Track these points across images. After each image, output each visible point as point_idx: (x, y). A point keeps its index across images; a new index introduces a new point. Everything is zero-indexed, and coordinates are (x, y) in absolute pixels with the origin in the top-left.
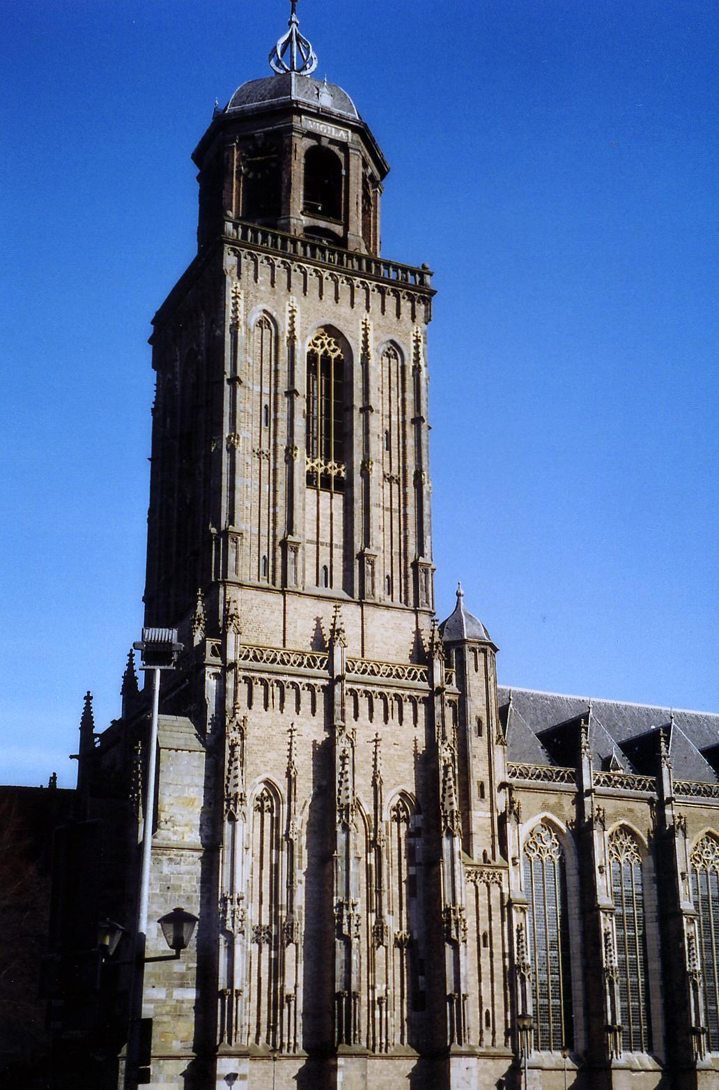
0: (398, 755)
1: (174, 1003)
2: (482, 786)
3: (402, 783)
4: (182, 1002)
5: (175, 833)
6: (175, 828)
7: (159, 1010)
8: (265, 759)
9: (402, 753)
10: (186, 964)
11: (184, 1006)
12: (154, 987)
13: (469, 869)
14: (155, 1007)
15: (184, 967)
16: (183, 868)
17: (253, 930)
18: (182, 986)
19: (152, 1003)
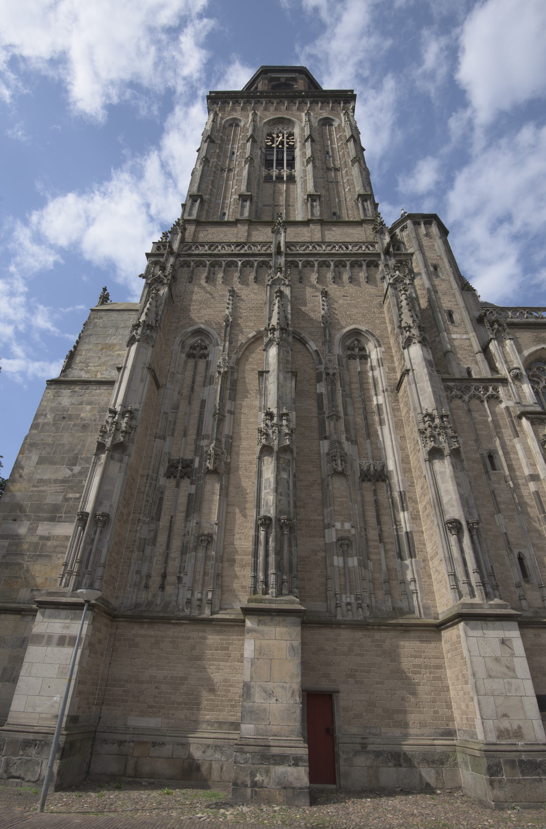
0: (348, 304)
1: (35, 539)
2: (450, 314)
3: (354, 323)
4: (48, 538)
5: (88, 372)
6: (89, 368)
7: (14, 548)
8: (200, 315)
9: (353, 302)
10: (63, 494)
11: (49, 543)
12: (15, 520)
13: (451, 384)
14: (9, 544)
15: (61, 498)
16: (86, 398)
17: (169, 462)
18: (52, 519)
19: (7, 539)
